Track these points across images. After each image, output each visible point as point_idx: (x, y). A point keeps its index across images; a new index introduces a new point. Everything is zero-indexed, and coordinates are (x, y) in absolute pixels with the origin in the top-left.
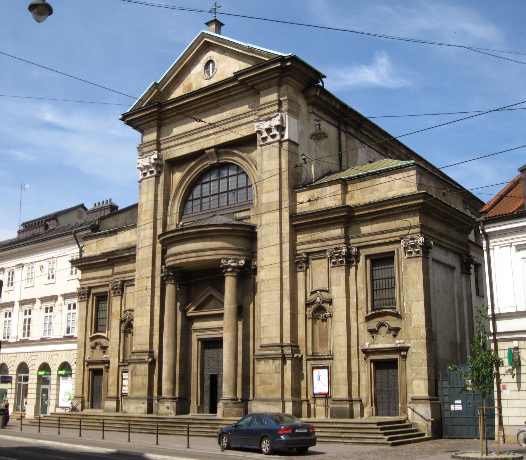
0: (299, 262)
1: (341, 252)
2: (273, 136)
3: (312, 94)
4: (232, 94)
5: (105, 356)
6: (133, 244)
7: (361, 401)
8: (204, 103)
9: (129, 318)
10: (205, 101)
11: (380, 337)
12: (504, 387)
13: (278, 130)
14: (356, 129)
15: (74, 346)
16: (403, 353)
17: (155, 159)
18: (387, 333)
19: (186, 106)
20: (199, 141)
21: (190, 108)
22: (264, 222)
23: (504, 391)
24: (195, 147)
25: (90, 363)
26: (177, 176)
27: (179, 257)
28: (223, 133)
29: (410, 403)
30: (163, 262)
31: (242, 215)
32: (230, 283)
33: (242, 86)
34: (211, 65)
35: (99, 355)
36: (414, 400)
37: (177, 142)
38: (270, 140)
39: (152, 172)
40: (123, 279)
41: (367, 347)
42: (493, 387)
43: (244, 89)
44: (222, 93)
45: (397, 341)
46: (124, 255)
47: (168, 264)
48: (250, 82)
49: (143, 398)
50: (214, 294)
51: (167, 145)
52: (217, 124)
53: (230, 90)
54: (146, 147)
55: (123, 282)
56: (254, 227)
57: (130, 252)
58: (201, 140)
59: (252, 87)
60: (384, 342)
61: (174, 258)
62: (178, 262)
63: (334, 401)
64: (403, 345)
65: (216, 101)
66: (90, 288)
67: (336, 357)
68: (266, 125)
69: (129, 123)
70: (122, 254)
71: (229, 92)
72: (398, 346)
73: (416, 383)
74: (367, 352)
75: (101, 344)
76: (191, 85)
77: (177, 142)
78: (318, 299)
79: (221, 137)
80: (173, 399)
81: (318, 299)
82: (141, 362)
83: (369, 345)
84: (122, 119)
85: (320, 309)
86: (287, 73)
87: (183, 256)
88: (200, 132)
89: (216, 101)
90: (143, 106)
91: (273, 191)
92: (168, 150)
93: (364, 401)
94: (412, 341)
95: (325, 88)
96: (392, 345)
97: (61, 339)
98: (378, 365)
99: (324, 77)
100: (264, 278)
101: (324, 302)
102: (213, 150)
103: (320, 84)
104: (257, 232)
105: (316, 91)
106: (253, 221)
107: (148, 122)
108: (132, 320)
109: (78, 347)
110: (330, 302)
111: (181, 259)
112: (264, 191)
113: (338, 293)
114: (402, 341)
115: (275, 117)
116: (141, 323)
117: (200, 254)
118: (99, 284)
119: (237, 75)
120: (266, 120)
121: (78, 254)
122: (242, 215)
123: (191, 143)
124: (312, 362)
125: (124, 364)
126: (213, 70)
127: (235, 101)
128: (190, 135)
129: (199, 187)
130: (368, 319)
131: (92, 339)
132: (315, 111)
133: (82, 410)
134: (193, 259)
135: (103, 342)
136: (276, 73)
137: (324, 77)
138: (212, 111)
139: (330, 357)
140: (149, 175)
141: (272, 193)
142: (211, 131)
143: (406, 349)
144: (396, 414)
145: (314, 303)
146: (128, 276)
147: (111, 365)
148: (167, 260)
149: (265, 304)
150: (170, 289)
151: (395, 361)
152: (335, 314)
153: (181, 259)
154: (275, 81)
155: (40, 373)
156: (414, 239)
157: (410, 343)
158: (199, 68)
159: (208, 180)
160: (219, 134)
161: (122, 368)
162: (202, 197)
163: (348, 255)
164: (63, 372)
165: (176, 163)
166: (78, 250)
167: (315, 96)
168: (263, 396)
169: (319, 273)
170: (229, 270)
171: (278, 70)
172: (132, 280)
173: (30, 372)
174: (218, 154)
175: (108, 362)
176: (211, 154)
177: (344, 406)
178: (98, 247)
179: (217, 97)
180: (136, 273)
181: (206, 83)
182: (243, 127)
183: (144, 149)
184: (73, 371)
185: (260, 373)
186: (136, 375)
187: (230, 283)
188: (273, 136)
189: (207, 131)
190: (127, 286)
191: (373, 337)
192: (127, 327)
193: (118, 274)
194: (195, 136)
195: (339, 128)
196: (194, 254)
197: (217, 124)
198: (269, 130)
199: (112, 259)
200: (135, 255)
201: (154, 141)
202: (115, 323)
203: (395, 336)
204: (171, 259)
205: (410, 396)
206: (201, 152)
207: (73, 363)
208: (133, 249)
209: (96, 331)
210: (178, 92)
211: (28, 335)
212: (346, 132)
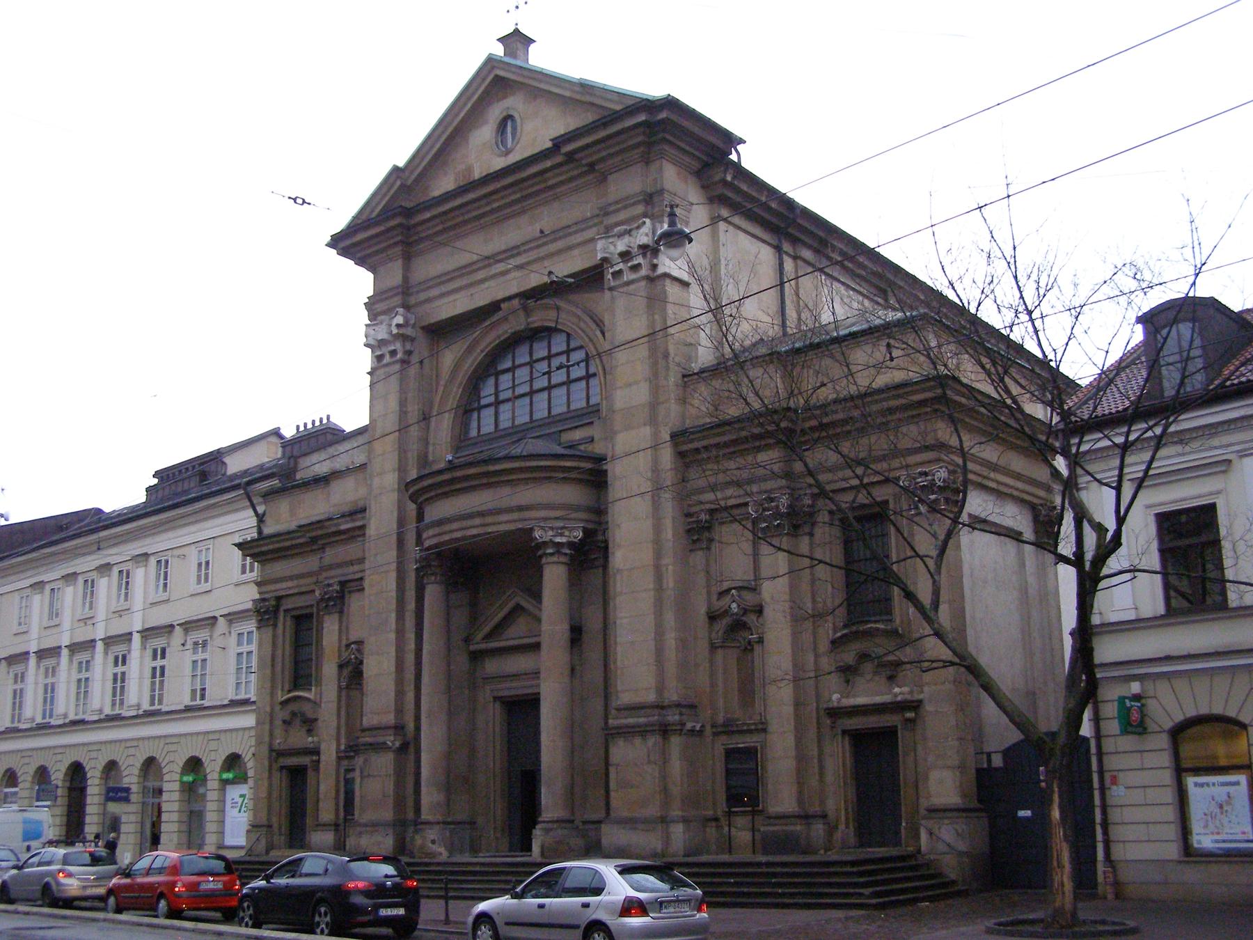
0: (699, 531)
1: (777, 507)
2: (636, 268)
3: (717, 178)
4: (550, 183)
5: (310, 739)
6: (361, 504)
7: (824, 816)
8: (495, 205)
10: (498, 200)
11: (860, 683)
12: (1114, 781)
13: (644, 255)
14: (817, 251)
15: (249, 720)
16: (910, 715)
17: (398, 326)
18: (875, 673)
19: (457, 212)
20: (487, 284)
22: (619, 449)
23: (1115, 787)
24: (481, 298)
25: (281, 754)
26: (448, 358)
27: (447, 528)
29: (925, 818)
30: (419, 541)
31: (577, 435)
32: (554, 576)
33: (571, 166)
34: (509, 124)
35: (299, 738)
36: (933, 811)
37: (443, 289)
38: (628, 276)
39: (393, 353)
40: (343, 579)
41: (835, 704)
42: (1091, 781)
43: (576, 172)
44: (530, 182)
45: (897, 690)
46: (343, 527)
47: (427, 544)
49: (386, 824)
50: (524, 604)
51: (422, 296)
52: (522, 248)
53: (548, 175)
55: (343, 584)
56: (601, 459)
57: (353, 521)
58: (492, 283)
59: (592, 166)
60: (869, 692)
62: (446, 537)
63: (770, 818)
64: (909, 697)
66: (279, 599)
67: (774, 726)
68: (621, 246)
69: (345, 252)
70: (338, 525)
71: (545, 181)
72: (899, 698)
73: (934, 775)
74: (835, 713)
75: (303, 714)
76: (469, 169)
77: (443, 289)
78: (734, 605)
80: (445, 823)
81: (734, 605)
82: (379, 747)
83: (839, 700)
84: (330, 245)
85: (738, 626)
86: (661, 135)
87: (455, 526)
88: (489, 265)
90: (374, 215)
91: (637, 383)
92: (427, 306)
93: (831, 815)
94: (926, 689)
95: (743, 165)
96: (887, 698)
97: (224, 706)
98: (859, 739)
99: (742, 141)
100: (621, 566)
101: (745, 611)
102: (516, 302)
103: (734, 157)
104: (606, 471)
105: (725, 172)
106: (598, 448)
108: (361, 663)
109: (258, 723)
110: (759, 610)
111: (451, 531)
112: (619, 384)
113: (774, 592)
114: (906, 689)
115: (638, 228)
116: (380, 668)
117: (489, 519)
119: (558, 143)
120: (620, 235)
121: (255, 530)
122: (577, 435)
123: (472, 291)
124: (723, 738)
125: (351, 750)
126: (514, 135)
127: (557, 198)
129: (491, 381)
130: (836, 643)
131: (284, 703)
132: (725, 213)
133: (267, 852)
134: (474, 532)
135: (307, 709)
137: (742, 141)
139: (760, 727)
140: (387, 359)
141: (635, 387)
143: (916, 706)
144: (898, 843)
145: (726, 612)
146: (351, 572)
147: (323, 758)
148: (425, 536)
149: (625, 621)
150: (433, 592)
151: (891, 732)
152: (770, 637)
153: (451, 531)
154: (636, 154)
155: (186, 779)
156: (926, 474)
157: (922, 692)
158: (484, 134)
159: (507, 364)
161: (345, 762)
162: (498, 403)
163: (793, 512)
164: (230, 775)
165: (440, 332)
166: (253, 521)
167: (724, 182)
168: (625, 814)
169: (735, 554)
170: (550, 551)
171: (641, 129)
172: (361, 579)
173: (166, 778)
174: (527, 311)
175: (316, 752)
177: (791, 828)
178: (292, 512)
179: (521, 190)
180: (367, 565)
181: (499, 163)
182: (576, 252)
184: (251, 773)
185: (618, 765)
186: (369, 776)
187: (554, 576)
188: (636, 268)
190: (350, 592)
191: (848, 682)
192: (353, 674)
193: (331, 567)
194: (481, 275)
195: (778, 249)
196: (477, 521)
197: (522, 248)
198: (625, 256)
199: (316, 537)
200: (363, 527)
201: (397, 287)
202: (329, 670)
203: (891, 678)
204: (431, 532)
205: (924, 803)
206: (495, 307)
207: (250, 755)
208: (359, 516)
209: (296, 685)
210: (445, 183)
211: (160, 702)
212: (795, 258)
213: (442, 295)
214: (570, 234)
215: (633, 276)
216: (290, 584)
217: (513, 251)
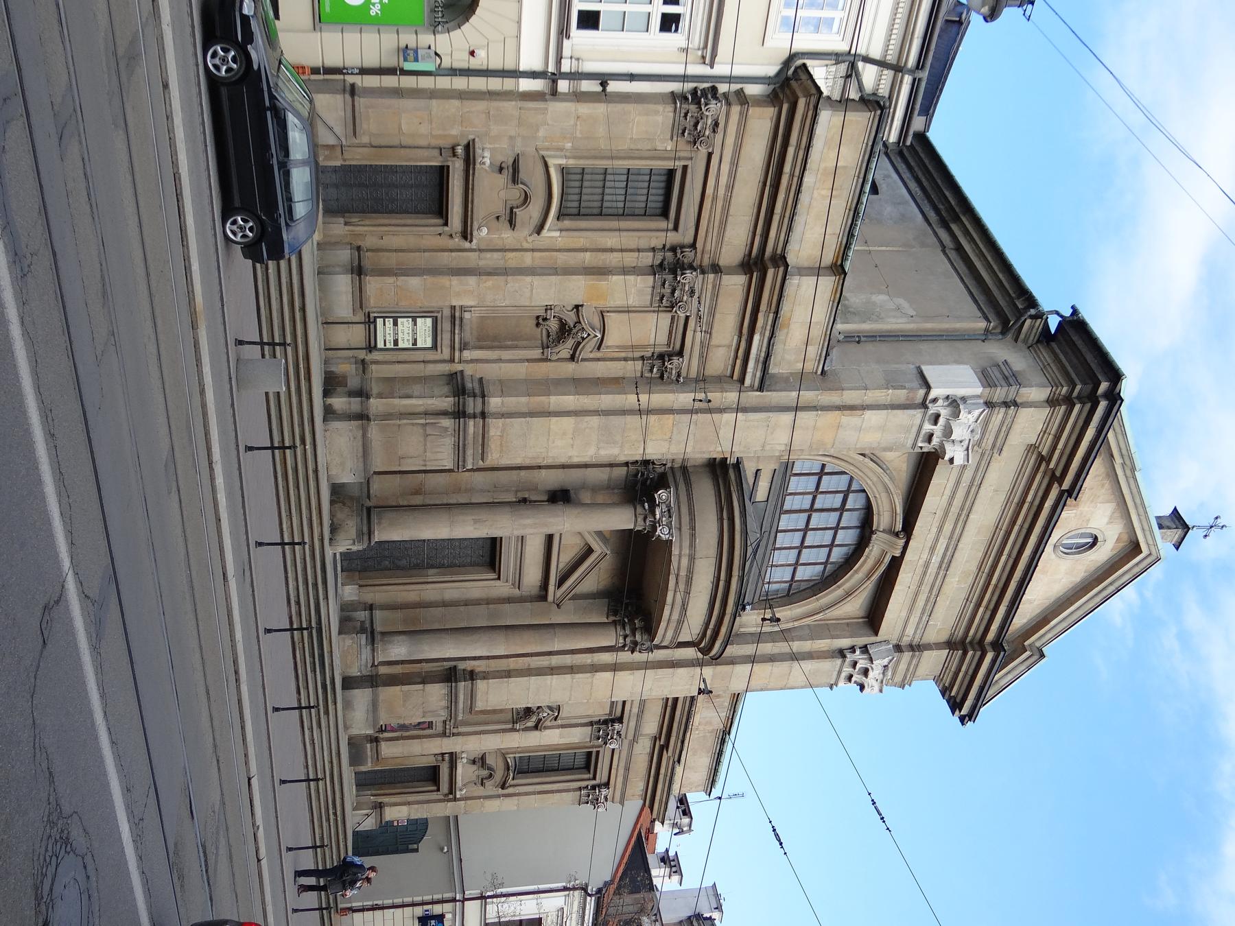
4: (981, 610)
8: (1004, 558)
9: (583, 339)
17: (951, 461)
20: (934, 530)
21: (1016, 528)
28: (917, 578)
46: (756, 338)
48: (973, 656)
54: (1003, 423)
61: (683, 573)
65: (991, 575)
70: (762, 335)
79: (910, 575)
88: (951, 538)
89: (991, 575)
107: (1057, 438)
118: (709, 191)
123: (940, 514)
128: (959, 515)
136: (958, 693)
138: (980, 555)
140: (928, 427)
142: (936, 560)
160: (919, 571)
176: (893, 545)
182: (904, 614)
183: (1000, 416)
189: (942, 551)
194: (948, 527)
198: (865, 672)
213: (958, 483)
214: (923, 613)
215: (843, 675)
216: (724, 180)
217: (946, 564)
